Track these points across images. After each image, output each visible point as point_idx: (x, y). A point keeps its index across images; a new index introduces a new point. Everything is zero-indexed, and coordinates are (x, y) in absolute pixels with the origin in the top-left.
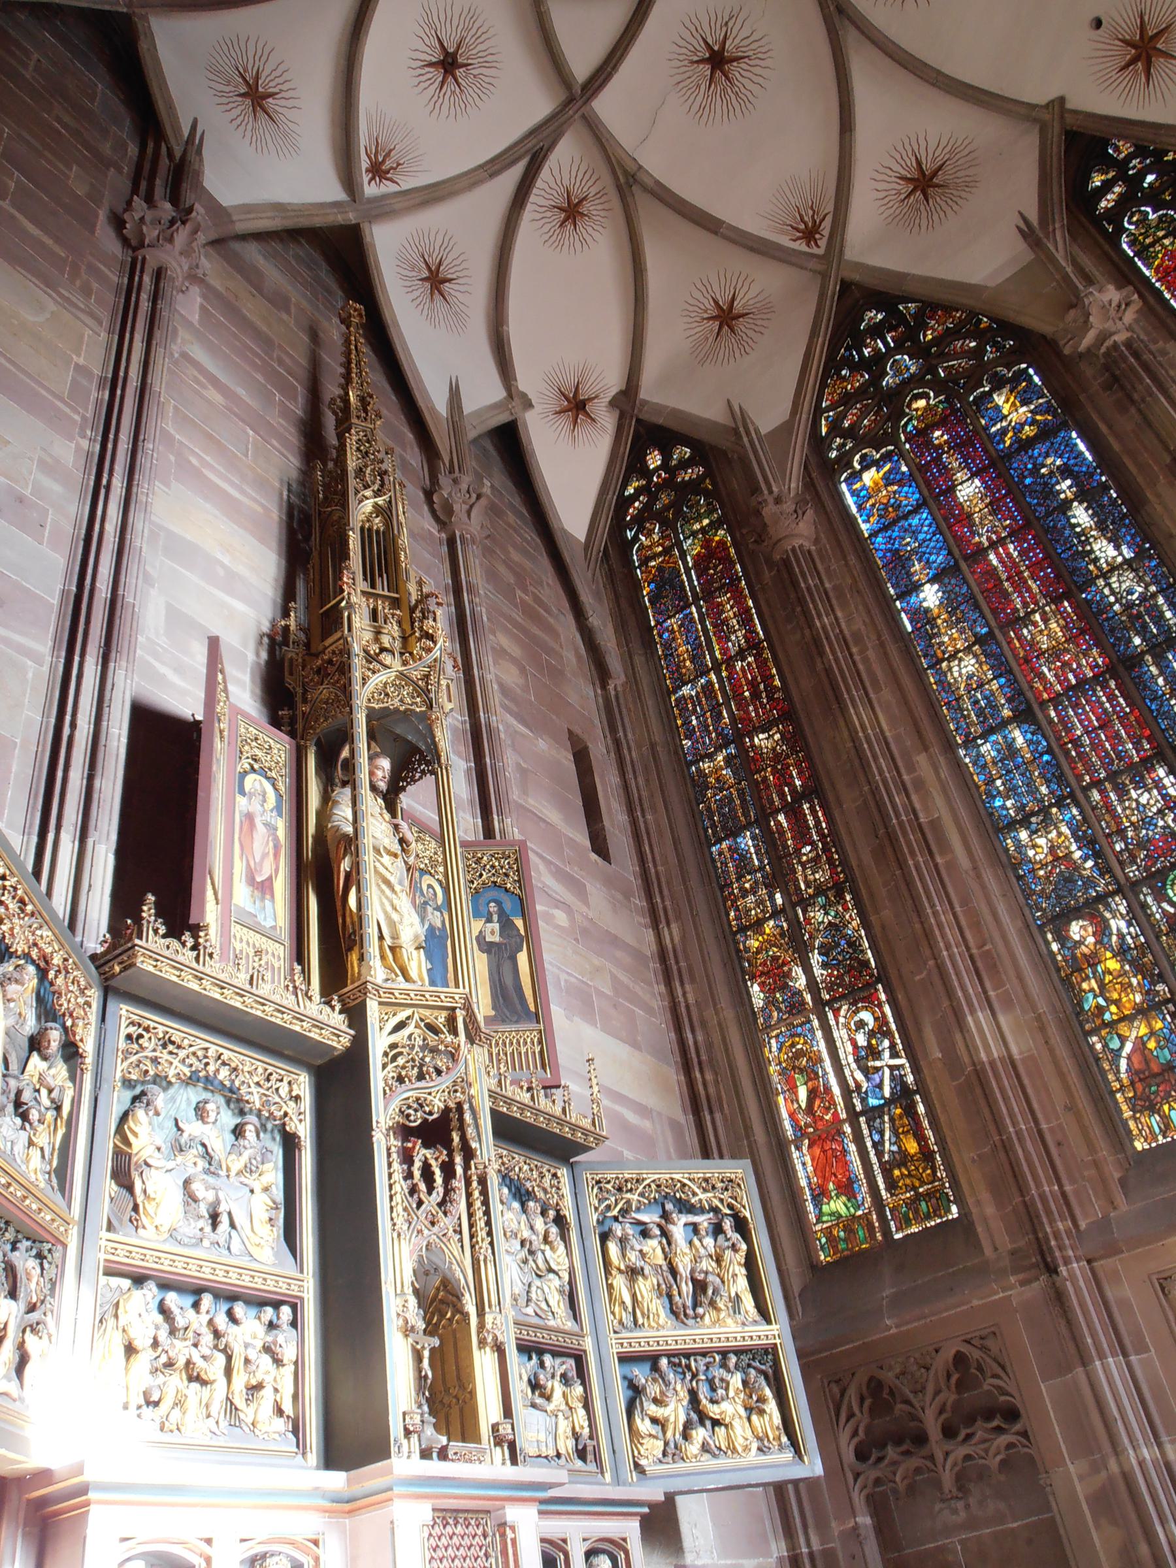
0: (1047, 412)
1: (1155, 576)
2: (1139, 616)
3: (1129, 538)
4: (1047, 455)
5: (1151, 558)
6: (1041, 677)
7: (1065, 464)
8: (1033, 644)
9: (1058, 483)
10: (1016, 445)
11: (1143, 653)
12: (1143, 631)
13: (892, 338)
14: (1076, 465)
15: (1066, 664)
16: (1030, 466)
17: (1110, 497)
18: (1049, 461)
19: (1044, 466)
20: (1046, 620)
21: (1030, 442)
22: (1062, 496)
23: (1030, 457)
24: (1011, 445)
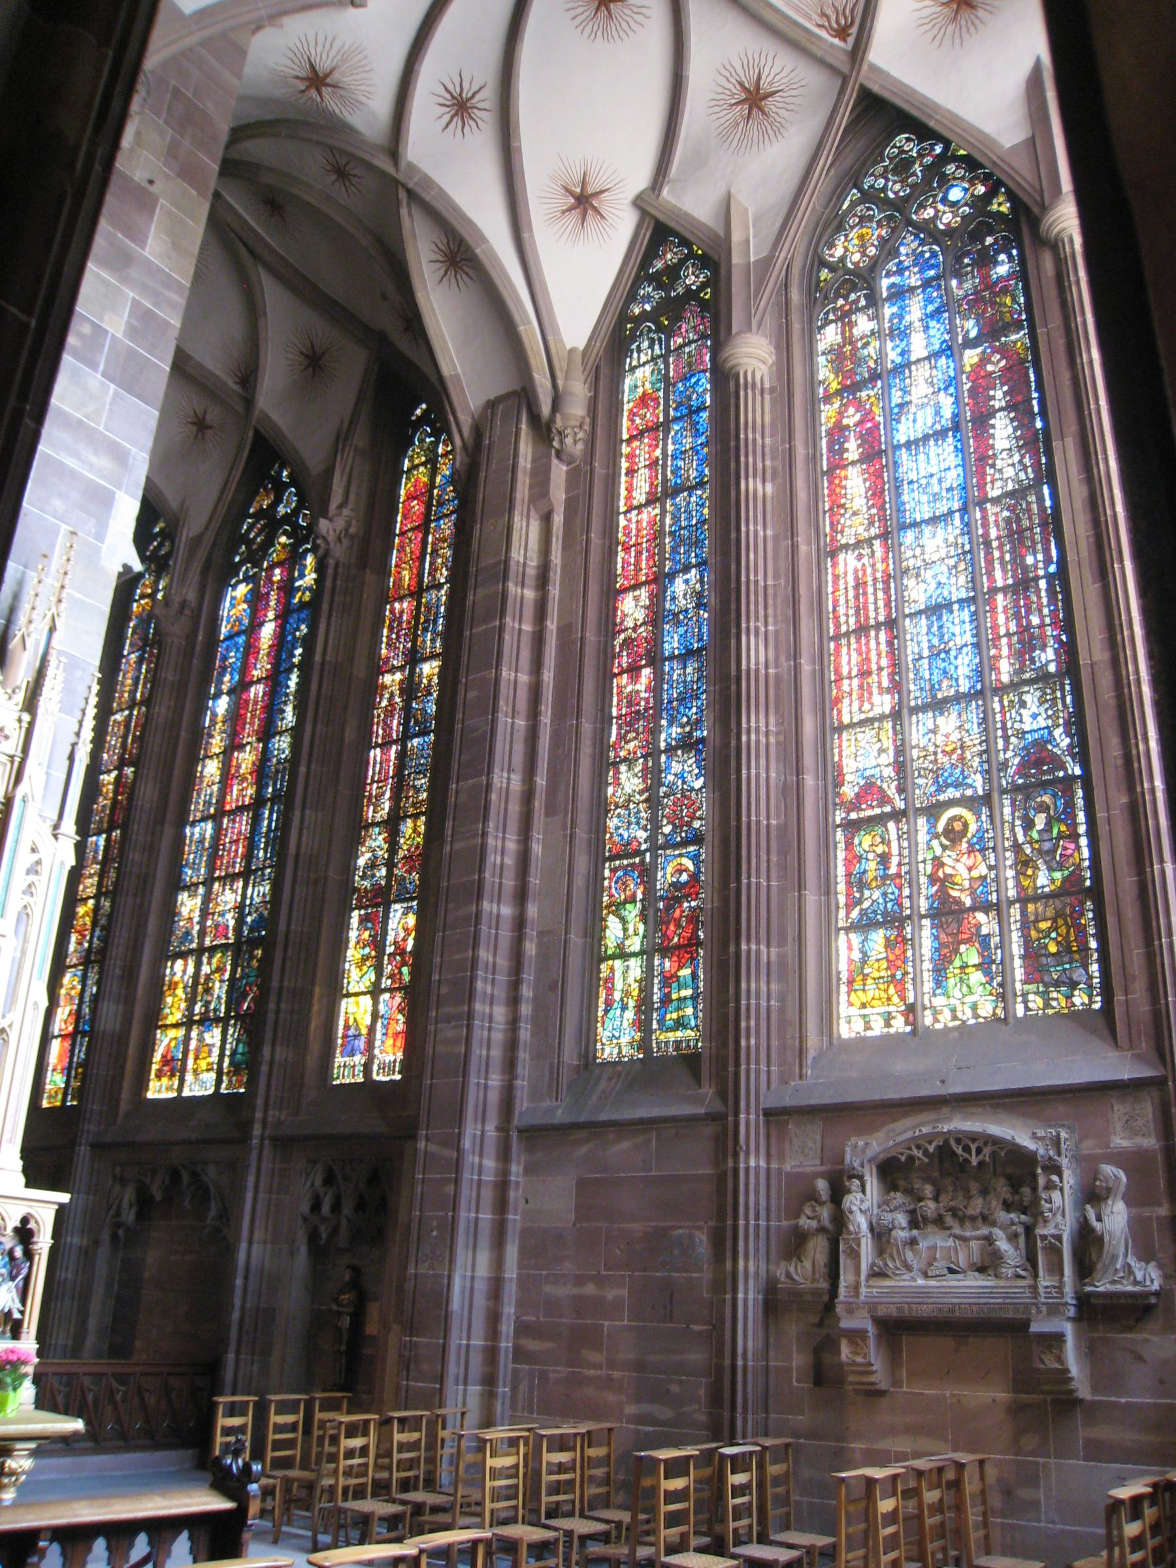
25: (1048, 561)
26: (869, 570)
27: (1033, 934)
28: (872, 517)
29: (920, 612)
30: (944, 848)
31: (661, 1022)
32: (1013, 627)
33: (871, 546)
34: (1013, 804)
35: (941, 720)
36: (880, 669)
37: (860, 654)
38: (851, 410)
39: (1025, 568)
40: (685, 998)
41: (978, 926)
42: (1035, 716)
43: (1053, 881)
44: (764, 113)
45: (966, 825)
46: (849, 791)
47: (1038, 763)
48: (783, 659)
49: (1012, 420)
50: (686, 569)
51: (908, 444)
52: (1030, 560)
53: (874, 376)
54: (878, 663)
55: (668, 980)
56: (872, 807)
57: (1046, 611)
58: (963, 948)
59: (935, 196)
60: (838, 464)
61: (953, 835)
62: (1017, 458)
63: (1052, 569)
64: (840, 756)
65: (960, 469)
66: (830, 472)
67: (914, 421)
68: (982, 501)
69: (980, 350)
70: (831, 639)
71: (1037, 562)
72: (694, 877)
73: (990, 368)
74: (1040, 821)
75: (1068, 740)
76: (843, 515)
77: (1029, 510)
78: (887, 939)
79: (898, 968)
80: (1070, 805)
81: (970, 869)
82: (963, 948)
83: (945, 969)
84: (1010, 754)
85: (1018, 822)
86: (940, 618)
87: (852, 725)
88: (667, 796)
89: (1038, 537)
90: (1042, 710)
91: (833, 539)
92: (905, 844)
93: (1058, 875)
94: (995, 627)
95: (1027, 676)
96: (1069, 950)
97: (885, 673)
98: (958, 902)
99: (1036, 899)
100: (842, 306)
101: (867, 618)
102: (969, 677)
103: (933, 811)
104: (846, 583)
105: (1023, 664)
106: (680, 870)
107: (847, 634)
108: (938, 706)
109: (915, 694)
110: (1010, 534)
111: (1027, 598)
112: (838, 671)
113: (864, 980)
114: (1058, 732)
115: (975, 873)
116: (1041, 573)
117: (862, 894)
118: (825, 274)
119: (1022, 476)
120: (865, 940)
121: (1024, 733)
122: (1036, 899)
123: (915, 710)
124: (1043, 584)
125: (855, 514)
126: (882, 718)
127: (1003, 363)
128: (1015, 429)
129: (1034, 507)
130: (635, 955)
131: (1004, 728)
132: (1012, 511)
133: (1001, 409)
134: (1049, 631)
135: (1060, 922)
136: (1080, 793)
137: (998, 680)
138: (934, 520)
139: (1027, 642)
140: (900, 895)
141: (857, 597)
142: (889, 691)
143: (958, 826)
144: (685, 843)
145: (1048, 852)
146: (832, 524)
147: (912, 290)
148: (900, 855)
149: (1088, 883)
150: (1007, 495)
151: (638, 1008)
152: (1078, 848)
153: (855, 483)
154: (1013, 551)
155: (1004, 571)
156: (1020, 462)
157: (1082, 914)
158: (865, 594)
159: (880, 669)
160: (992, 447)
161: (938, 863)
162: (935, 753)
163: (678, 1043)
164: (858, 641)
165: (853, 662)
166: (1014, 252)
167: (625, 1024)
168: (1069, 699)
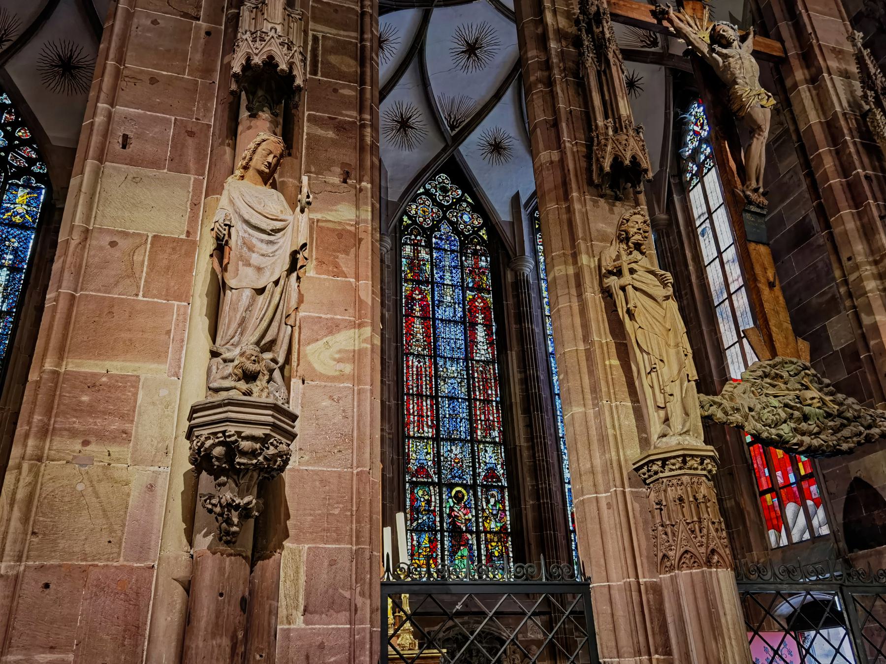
0: (32, 217)
1: (6, 326)
3: (11, 301)
4: (14, 237)
5: (11, 316)
7: (17, 247)
9: (7, 254)
10: (7, 221)
13: (6, 117)
14: (21, 251)
16: (4, 236)
17: (20, 277)
18: (13, 240)
19: (9, 241)
21: (12, 225)
22: (3, 261)
23: (8, 232)
24: (5, 219)
25: (496, 395)
26: (423, 369)
27: (490, 547)
28: (425, 345)
29: (446, 397)
30: (454, 503)
32: (483, 418)
33: (425, 359)
34: (482, 492)
35: (453, 448)
36: (428, 416)
37: (418, 406)
38: (417, 292)
39: (488, 395)
41: (468, 540)
42: (491, 458)
43: (497, 527)
44: (405, 133)
45: (463, 496)
46: (413, 467)
47: (492, 478)
48: (392, 399)
49: (485, 331)
51: (442, 320)
52: (490, 392)
53: (427, 282)
54: (427, 413)
56: (422, 477)
57: (495, 416)
58: (462, 548)
59: (457, 213)
60: (410, 314)
61: (458, 498)
62: (486, 347)
63: (498, 399)
64: (409, 448)
65: (463, 342)
66: (407, 316)
67: (445, 311)
68: (472, 359)
69: (473, 294)
70: (405, 394)
71: (492, 394)
73: (477, 304)
74: (492, 501)
75: (502, 471)
76: (412, 339)
78: (429, 538)
79: (434, 552)
80: (503, 497)
81: (465, 515)
82: (462, 548)
83: (455, 556)
84: (480, 470)
85: (484, 500)
86: (453, 402)
87: (413, 437)
89: (493, 384)
90: (493, 455)
91: (407, 348)
92: (438, 498)
93: (498, 525)
94: (476, 415)
95: (488, 440)
96: (502, 555)
97: (429, 418)
98: (460, 528)
99: (490, 532)
100: (413, 240)
101: (422, 391)
102: (465, 433)
103: (451, 486)
104: (413, 371)
105: (486, 435)
107: (413, 395)
108: (453, 441)
109: (443, 434)
110: (483, 378)
111: (488, 407)
112: (408, 410)
113: (419, 555)
114: (499, 466)
115: (467, 517)
116: (494, 399)
117: (418, 516)
118: (405, 218)
119: (487, 356)
120: (420, 537)
121: (486, 463)
122: (490, 532)
123: (443, 439)
124: (494, 404)
125: (417, 341)
126: (428, 438)
127: (482, 304)
128: (486, 335)
131: (479, 459)
132: (484, 369)
133: (480, 324)
134: (496, 424)
135: (499, 544)
136: (507, 494)
137: (477, 437)
138: (452, 359)
139: (489, 428)
140: (435, 520)
141: (417, 379)
142: (431, 427)
143: (460, 495)
145: (495, 515)
146: (406, 340)
147: (446, 251)
148: (435, 502)
149: (509, 530)
150: (481, 361)
152: (506, 515)
153: (418, 326)
154: (483, 385)
155: (480, 394)
156: (487, 349)
157: (507, 542)
158: (421, 379)
159: (428, 416)
160: (476, 338)
161: (451, 509)
162: (451, 461)
164: (418, 400)
165: (415, 409)
166: (489, 259)
168: (503, 454)
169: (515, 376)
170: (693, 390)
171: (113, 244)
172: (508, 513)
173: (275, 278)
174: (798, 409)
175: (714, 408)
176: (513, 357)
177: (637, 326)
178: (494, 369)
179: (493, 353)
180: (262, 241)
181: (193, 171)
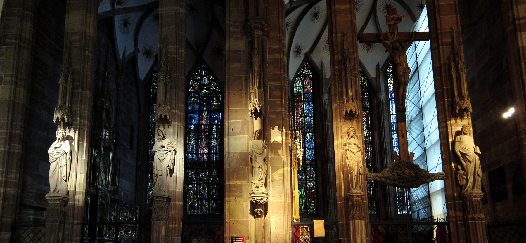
2: (214, 148)
6: (200, 149)
8: (201, 144)
11: (212, 153)
12: (214, 151)
15: (203, 149)
20: (204, 141)
25: (370, 150)
31: (309, 209)
39: (367, 150)
40: (313, 205)
50: (309, 132)
52: (368, 148)
55: (310, 202)
63: (371, 151)
72: (313, 186)
77: (368, 140)
88: (308, 172)
106: (311, 185)
124: (369, 153)
129: (369, 140)
130: (304, 197)
144: (311, 181)
151: (305, 206)
163: (312, 212)
167: (303, 208)
169: (377, 141)
170: (297, 203)
171: (234, 155)
172: (372, 192)
173: (261, 165)
174: (402, 176)
175: (377, 178)
176: (376, 134)
177: (349, 161)
178: (370, 139)
179: (369, 133)
180: (258, 156)
181: (246, 134)
